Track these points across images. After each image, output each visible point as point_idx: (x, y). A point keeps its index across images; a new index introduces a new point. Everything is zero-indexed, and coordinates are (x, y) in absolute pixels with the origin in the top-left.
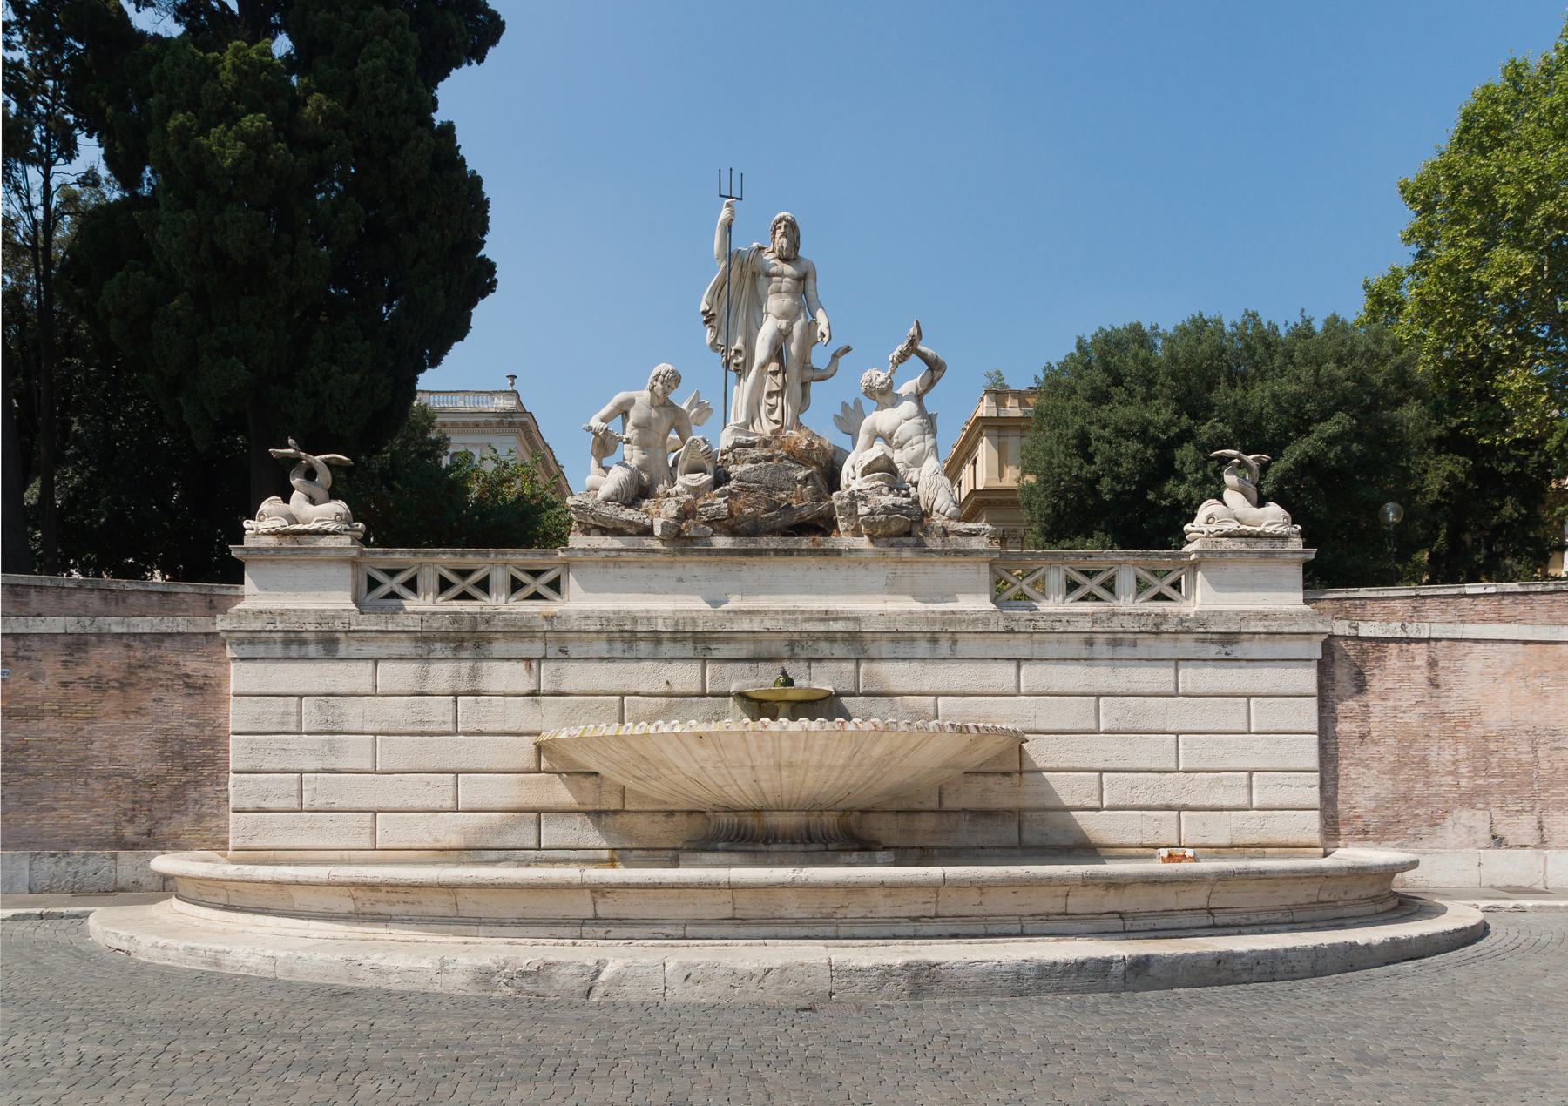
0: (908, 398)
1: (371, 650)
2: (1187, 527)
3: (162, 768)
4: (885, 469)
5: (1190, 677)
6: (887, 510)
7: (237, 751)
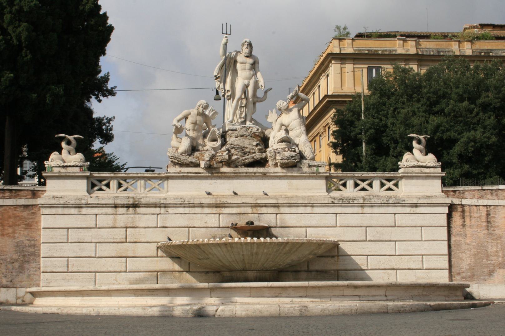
1: (96, 211)
2: (399, 163)
3: (16, 256)
4: (287, 140)
5: (401, 220)
7: (44, 250)
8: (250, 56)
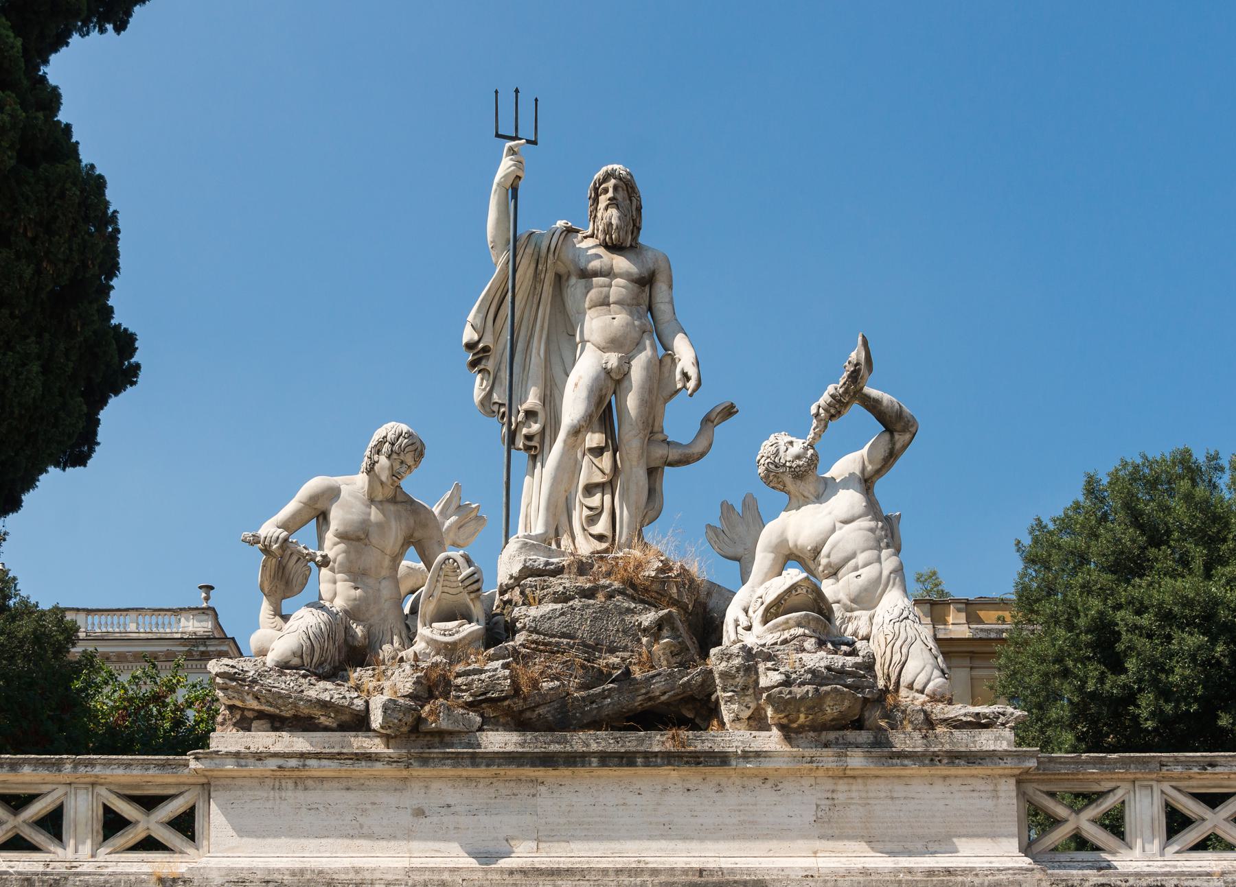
0: (846, 483)
6: (816, 677)
8: (622, 242)
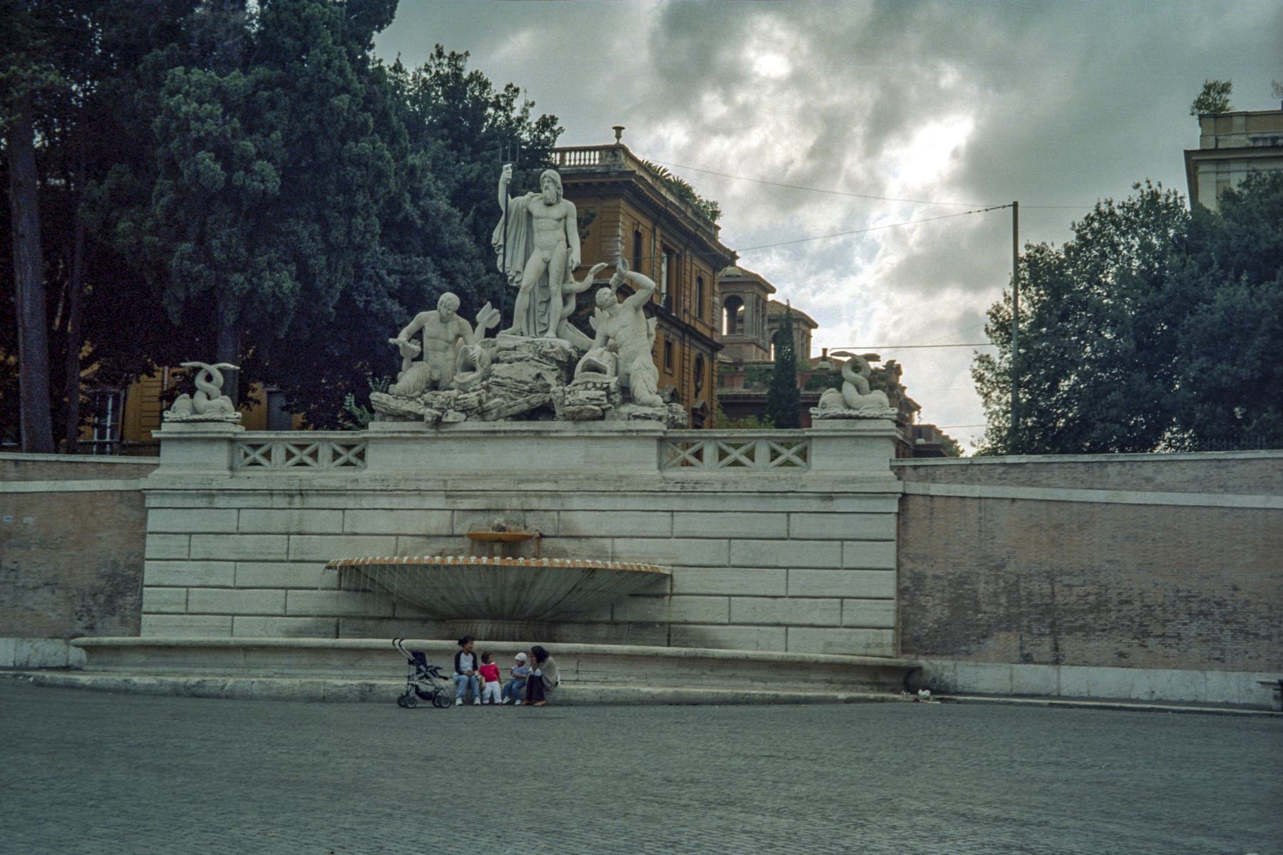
1: (237, 502)
3: (102, 583)
7: (151, 572)
